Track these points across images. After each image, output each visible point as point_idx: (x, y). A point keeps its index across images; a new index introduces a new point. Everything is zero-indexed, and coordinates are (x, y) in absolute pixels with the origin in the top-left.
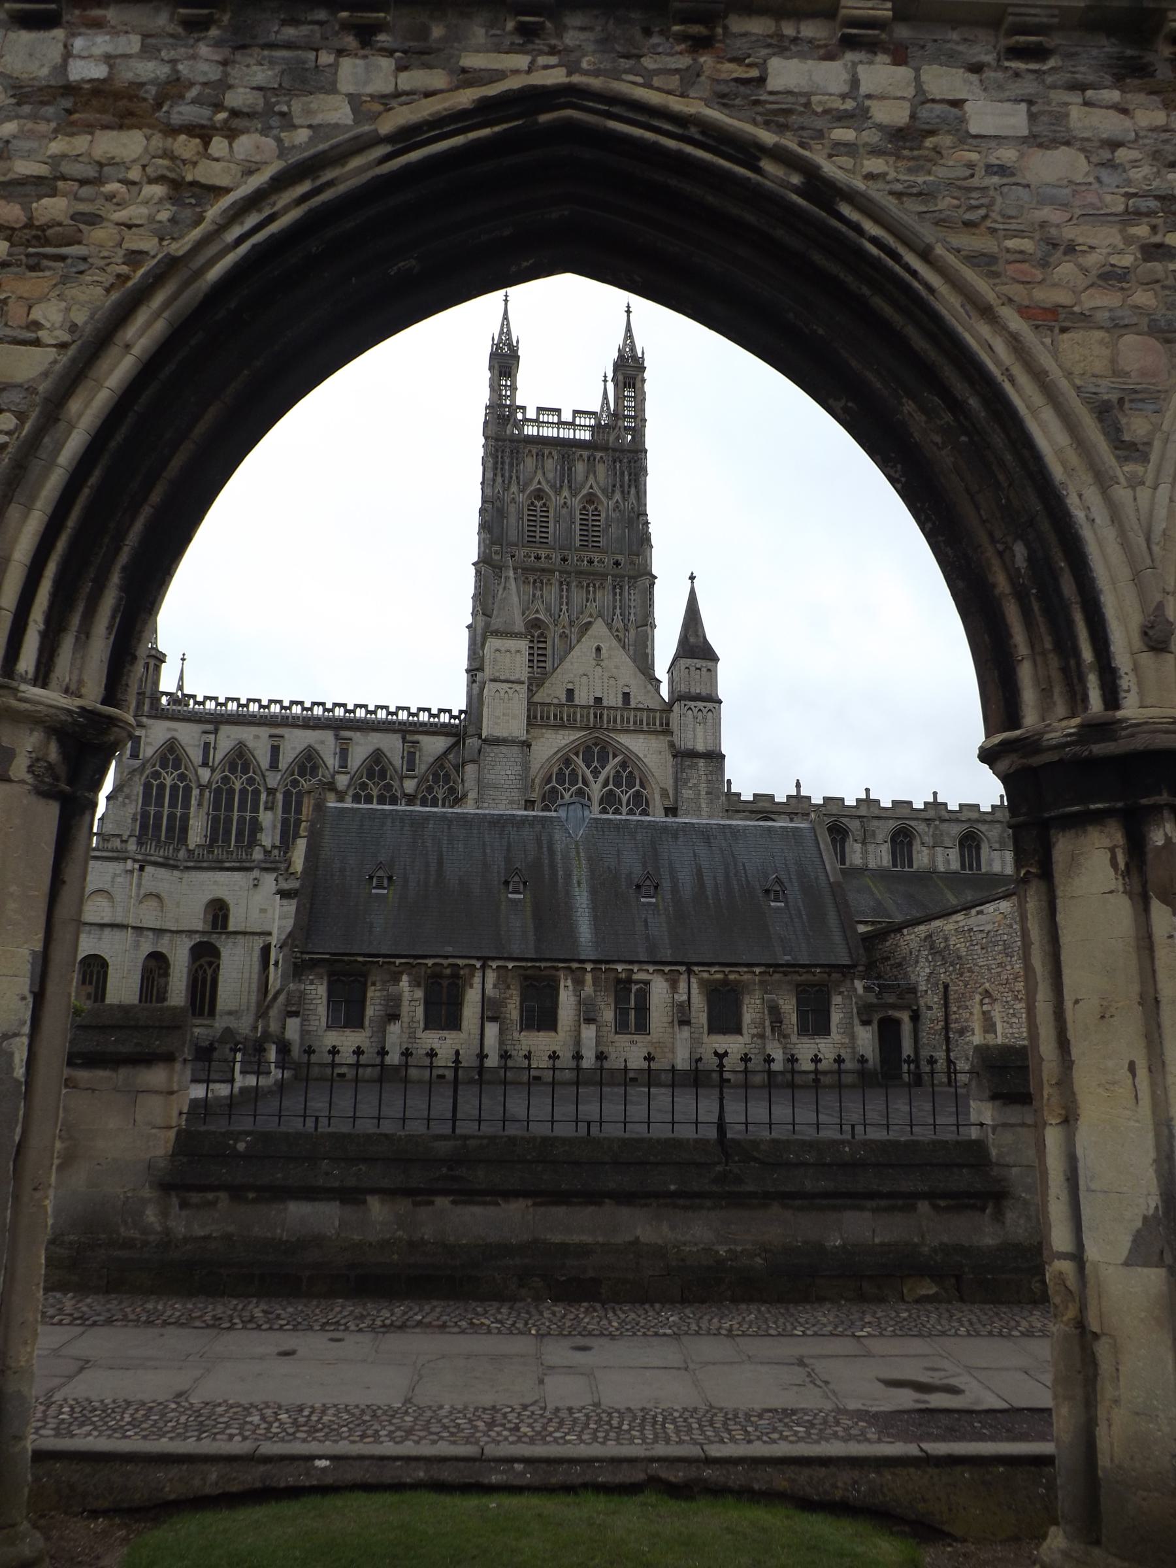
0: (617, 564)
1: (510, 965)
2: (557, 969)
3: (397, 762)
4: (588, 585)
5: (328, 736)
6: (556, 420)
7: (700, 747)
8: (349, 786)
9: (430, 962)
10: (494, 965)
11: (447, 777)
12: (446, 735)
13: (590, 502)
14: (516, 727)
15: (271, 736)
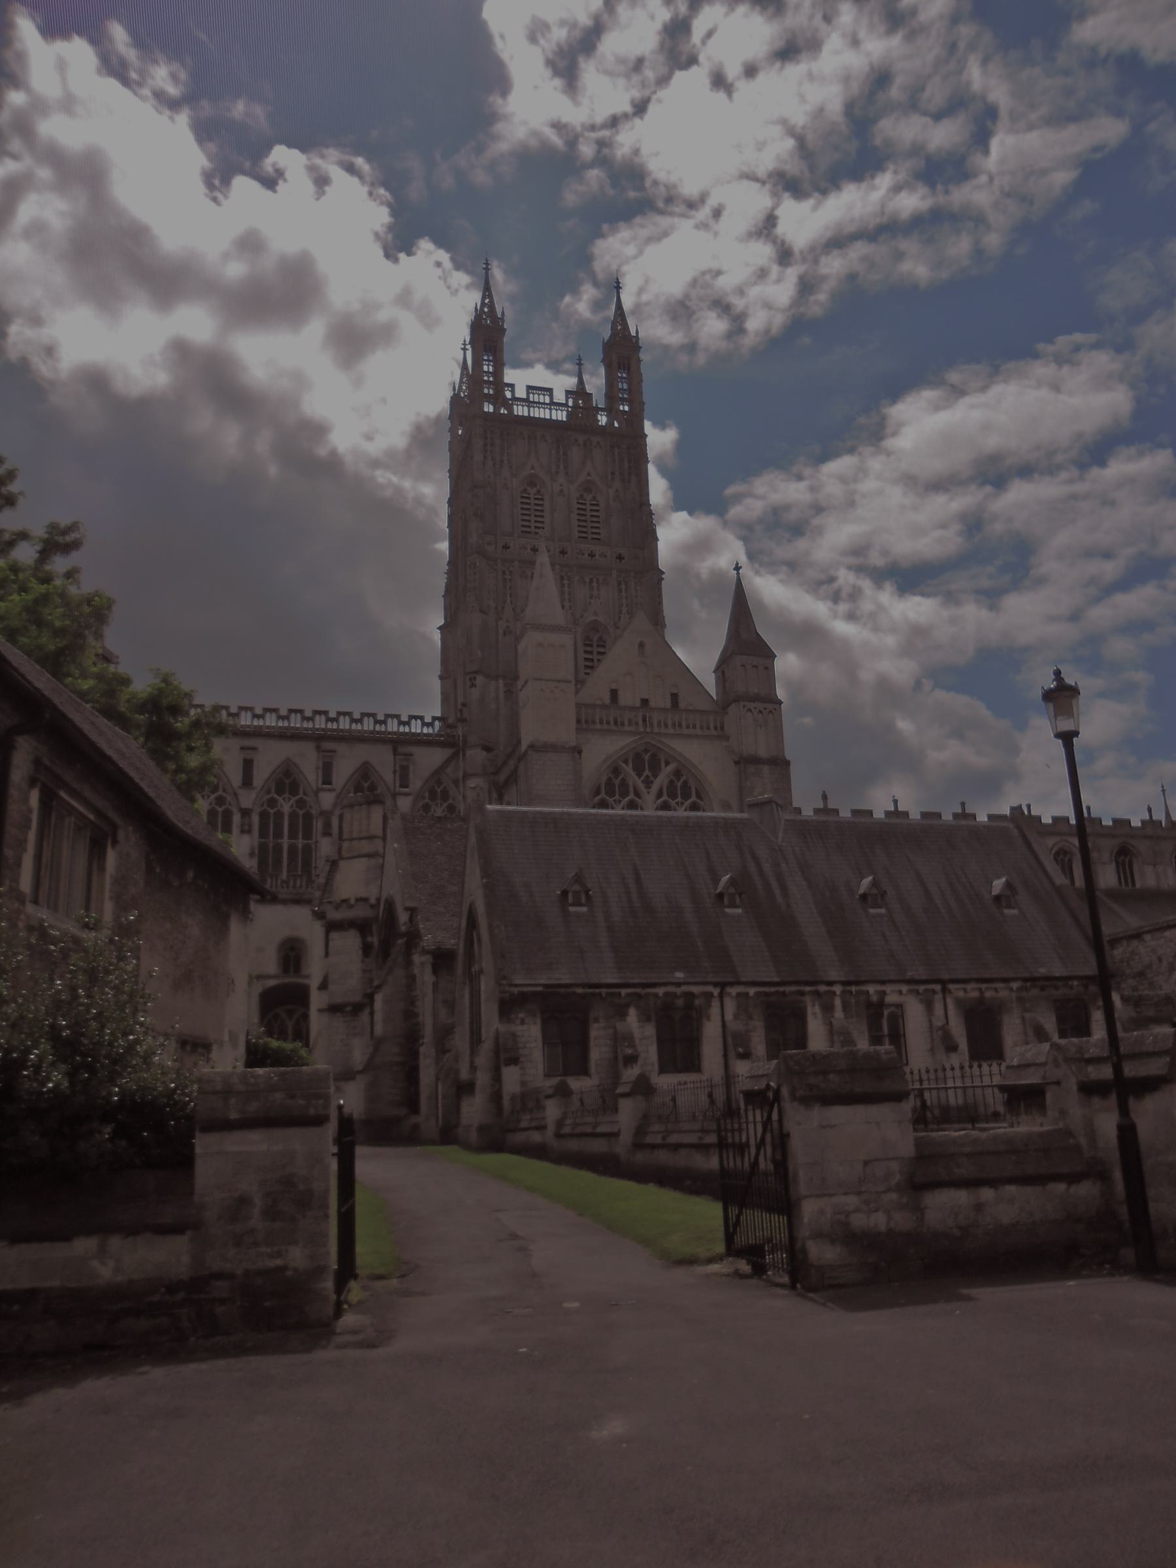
0: (620, 557)
1: (752, 991)
2: (802, 994)
3: (388, 776)
4: (591, 580)
5: (309, 748)
6: (547, 400)
7: (763, 753)
8: (335, 805)
9: (661, 991)
10: (733, 991)
11: (445, 795)
12: (442, 745)
13: (588, 490)
14: (566, 734)
15: (242, 748)
